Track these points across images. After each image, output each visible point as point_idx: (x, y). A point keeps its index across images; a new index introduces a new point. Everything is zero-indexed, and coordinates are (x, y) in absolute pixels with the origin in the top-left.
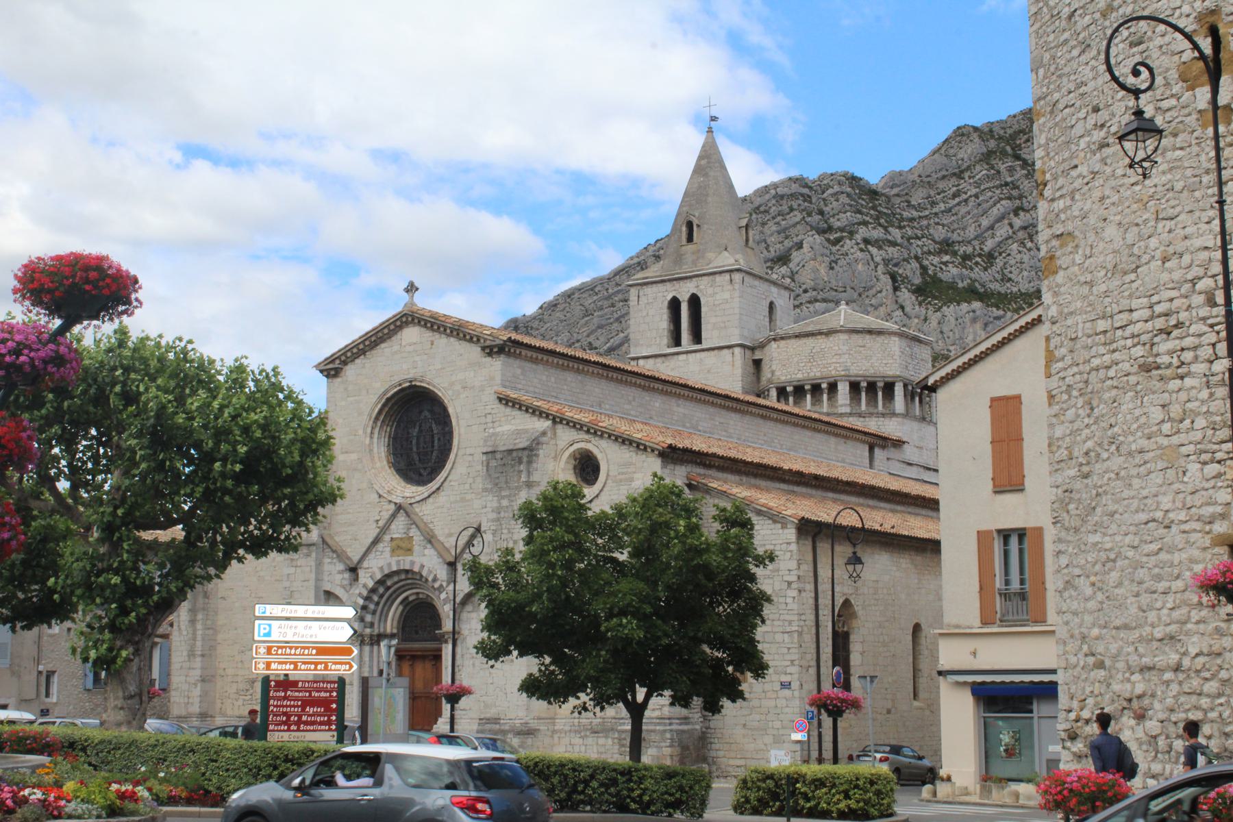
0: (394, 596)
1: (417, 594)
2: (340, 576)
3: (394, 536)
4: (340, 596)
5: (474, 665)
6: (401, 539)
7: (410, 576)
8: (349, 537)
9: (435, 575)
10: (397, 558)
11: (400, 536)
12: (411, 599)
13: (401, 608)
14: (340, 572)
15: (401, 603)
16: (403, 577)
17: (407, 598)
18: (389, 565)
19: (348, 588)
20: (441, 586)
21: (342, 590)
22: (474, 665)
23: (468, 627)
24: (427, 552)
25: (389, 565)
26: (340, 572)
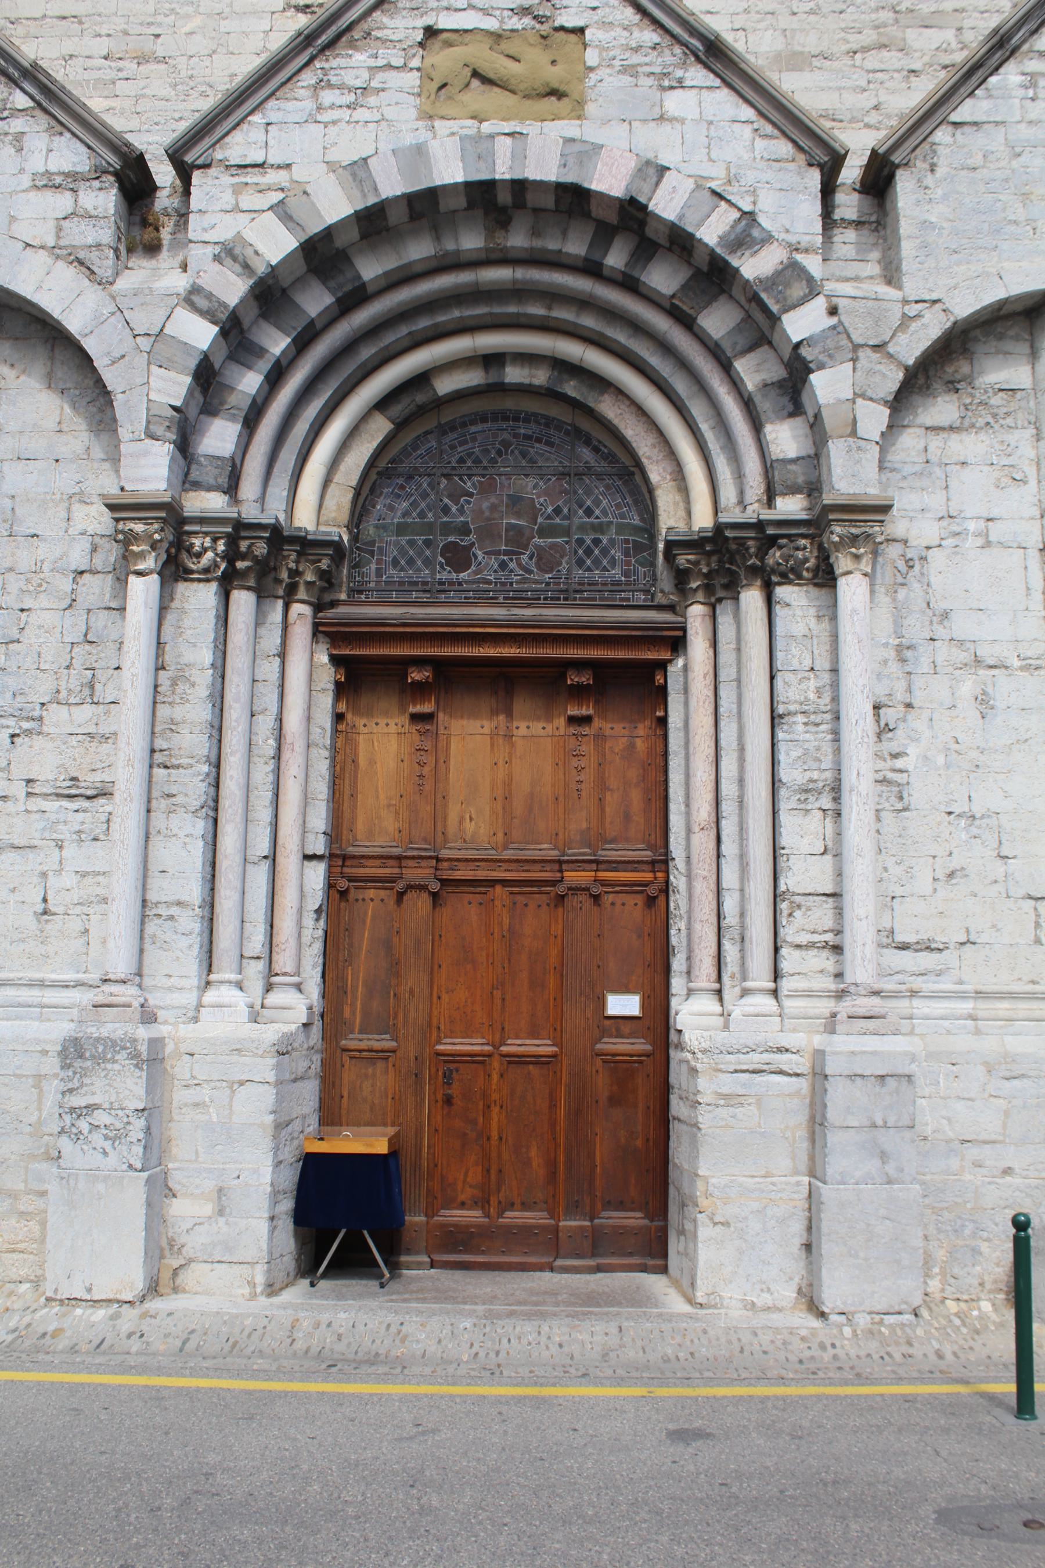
0: (367, 352)
1: (492, 360)
2: (63, 202)
3: (445, 21)
4: (50, 302)
5: (984, 701)
6: (497, 37)
7: (517, 240)
8: (102, 46)
9: (749, 217)
10: (469, 127)
11: (490, 24)
12: (445, 385)
13: (381, 427)
14: (48, 182)
15: (382, 404)
16: (471, 241)
17: (421, 380)
18: (420, 150)
19: (105, 264)
20: (792, 270)
21: (67, 274)
22: (984, 701)
23: (936, 501)
24: (675, 102)
25: (420, 150)
26: (48, 182)
